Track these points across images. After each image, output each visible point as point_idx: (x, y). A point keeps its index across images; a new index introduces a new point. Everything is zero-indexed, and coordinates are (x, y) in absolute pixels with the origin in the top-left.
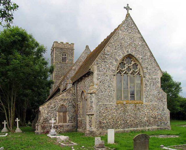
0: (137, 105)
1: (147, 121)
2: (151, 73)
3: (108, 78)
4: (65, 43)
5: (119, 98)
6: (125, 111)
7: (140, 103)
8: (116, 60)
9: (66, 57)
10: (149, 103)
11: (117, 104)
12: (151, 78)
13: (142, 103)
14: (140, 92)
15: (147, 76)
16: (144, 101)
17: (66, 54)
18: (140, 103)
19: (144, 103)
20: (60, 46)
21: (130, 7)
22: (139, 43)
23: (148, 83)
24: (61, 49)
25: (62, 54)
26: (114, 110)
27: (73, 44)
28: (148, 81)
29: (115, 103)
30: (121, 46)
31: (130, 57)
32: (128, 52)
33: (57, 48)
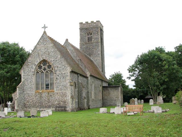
0: (50, 93)
1: (58, 104)
2: (61, 70)
3: (30, 77)
4: (89, 22)
5: (37, 88)
6: (41, 97)
7: (52, 92)
8: (35, 65)
9: (91, 37)
10: (59, 92)
11: (36, 92)
12: (61, 74)
13: (54, 92)
14: (52, 84)
15: (58, 72)
16: (55, 90)
17: (91, 34)
18: (52, 92)
19: (55, 91)
20: (85, 27)
21: (44, 26)
22: (52, 50)
23: (58, 77)
24: (86, 29)
25: (88, 34)
26: (34, 97)
27: (98, 21)
28: (58, 76)
29: (34, 92)
30: (38, 55)
31: (44, 62)
32: (43, 58)
33: (82, 29)
